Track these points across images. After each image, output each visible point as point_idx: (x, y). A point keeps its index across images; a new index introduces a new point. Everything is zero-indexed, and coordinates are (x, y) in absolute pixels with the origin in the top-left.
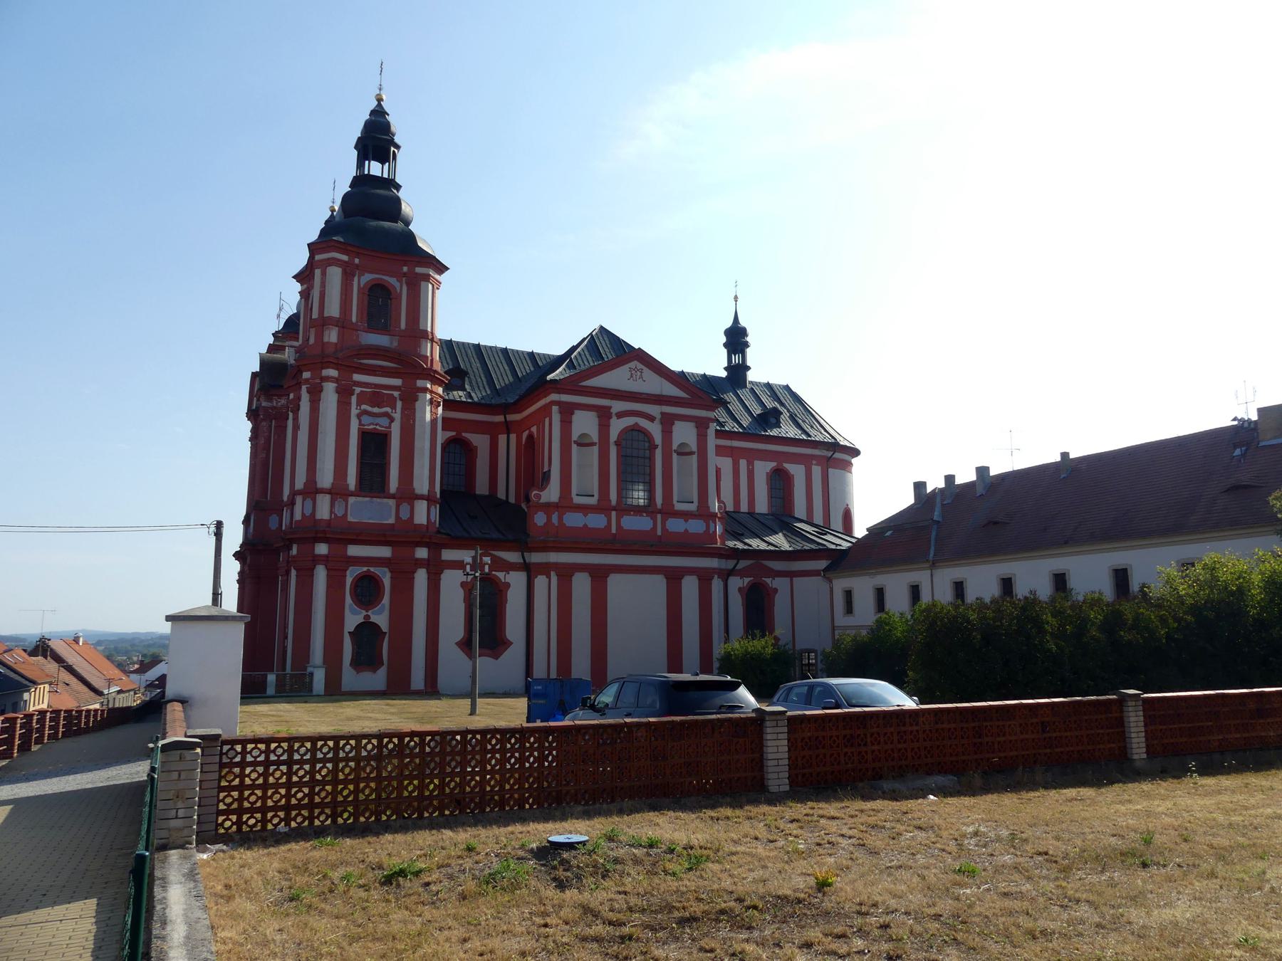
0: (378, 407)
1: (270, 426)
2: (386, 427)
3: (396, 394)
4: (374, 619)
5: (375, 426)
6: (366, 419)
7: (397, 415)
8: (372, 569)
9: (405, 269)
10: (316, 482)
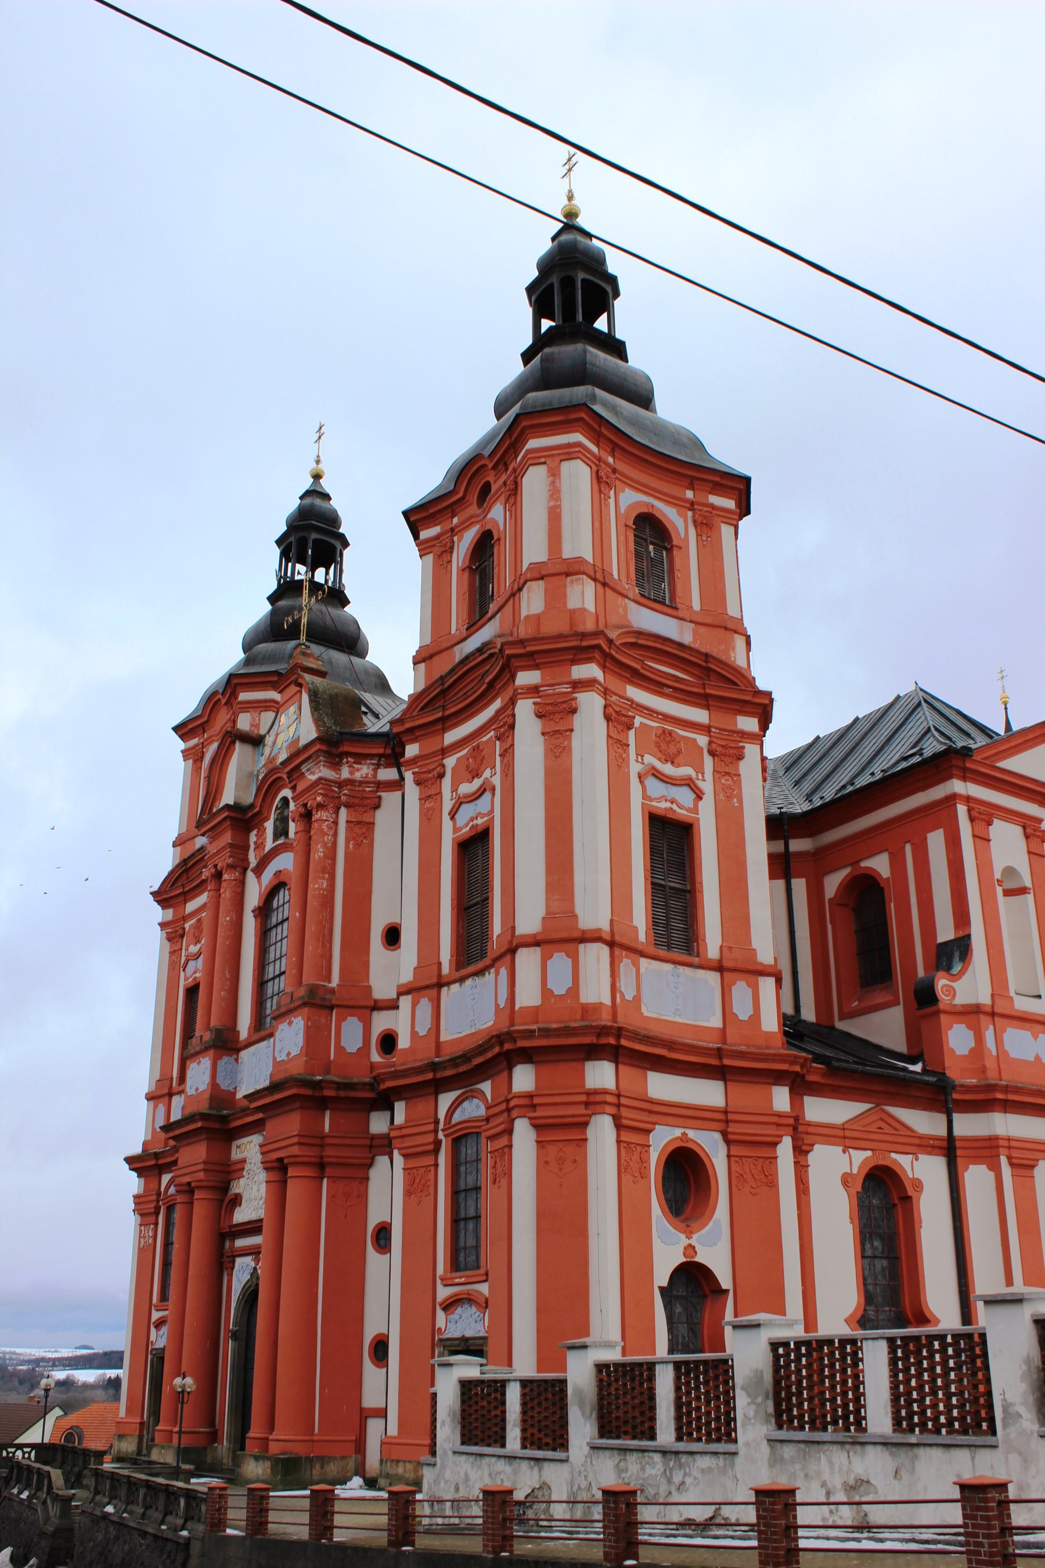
0: (672, 763)
1: (336, 823)
4: (702, 1257)
5: (668, 805)
6: (655, 787)
7: (707, 786)
8: (691, 1134)
9: (689, 494)
10: (575, 916)
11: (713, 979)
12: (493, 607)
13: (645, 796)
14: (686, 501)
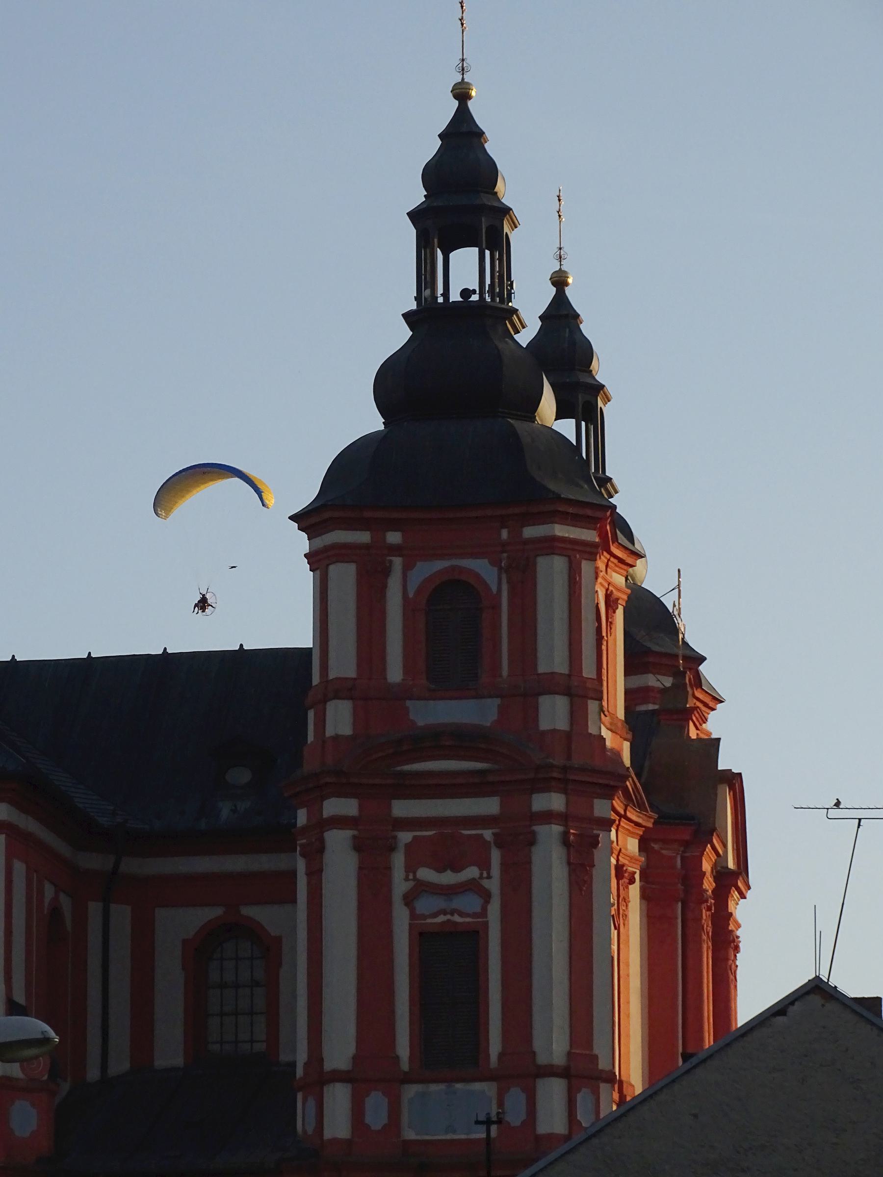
2: (475, 915)
3: (488, 834)
7: (494, 885)
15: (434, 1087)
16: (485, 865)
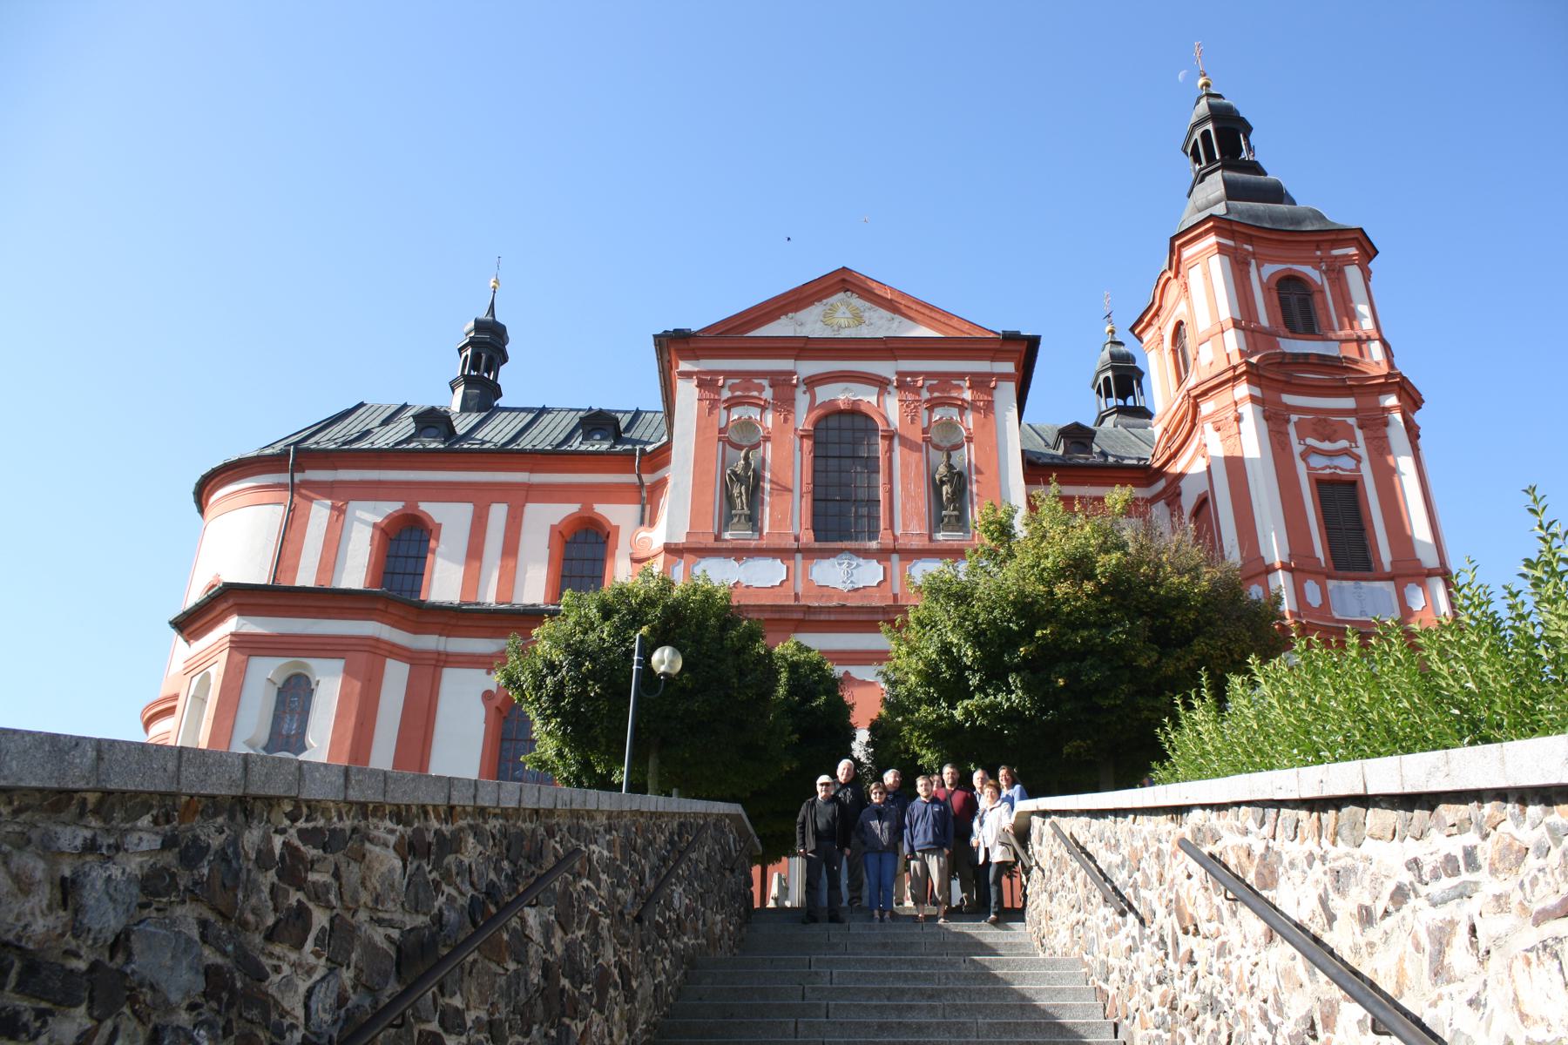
0: (1330, 440)
2: (1351, 471)
3: (1351, 421)
5: (1333, 470)
6: (1317, 461)
7: (1362, 450)
9: (1318, 253)
11: (1388, 587)
12: (1190, 370)
13: (1308, 467)
14: (1318, 257)
15: (1345, 583)
16: (1352, 439)
